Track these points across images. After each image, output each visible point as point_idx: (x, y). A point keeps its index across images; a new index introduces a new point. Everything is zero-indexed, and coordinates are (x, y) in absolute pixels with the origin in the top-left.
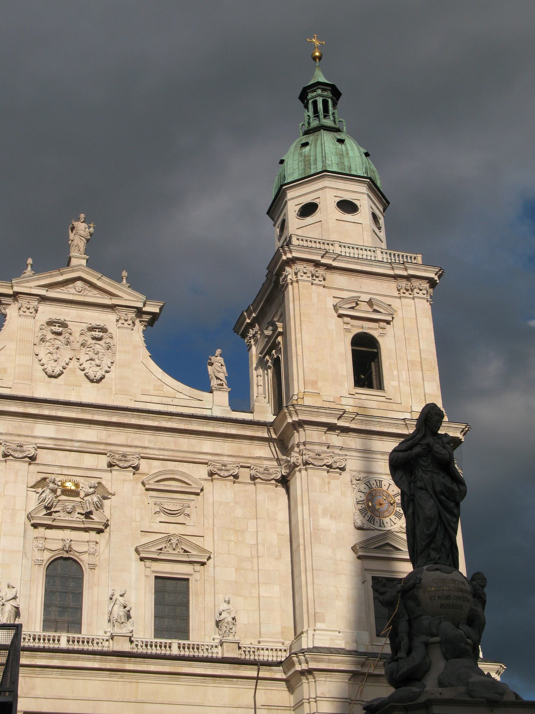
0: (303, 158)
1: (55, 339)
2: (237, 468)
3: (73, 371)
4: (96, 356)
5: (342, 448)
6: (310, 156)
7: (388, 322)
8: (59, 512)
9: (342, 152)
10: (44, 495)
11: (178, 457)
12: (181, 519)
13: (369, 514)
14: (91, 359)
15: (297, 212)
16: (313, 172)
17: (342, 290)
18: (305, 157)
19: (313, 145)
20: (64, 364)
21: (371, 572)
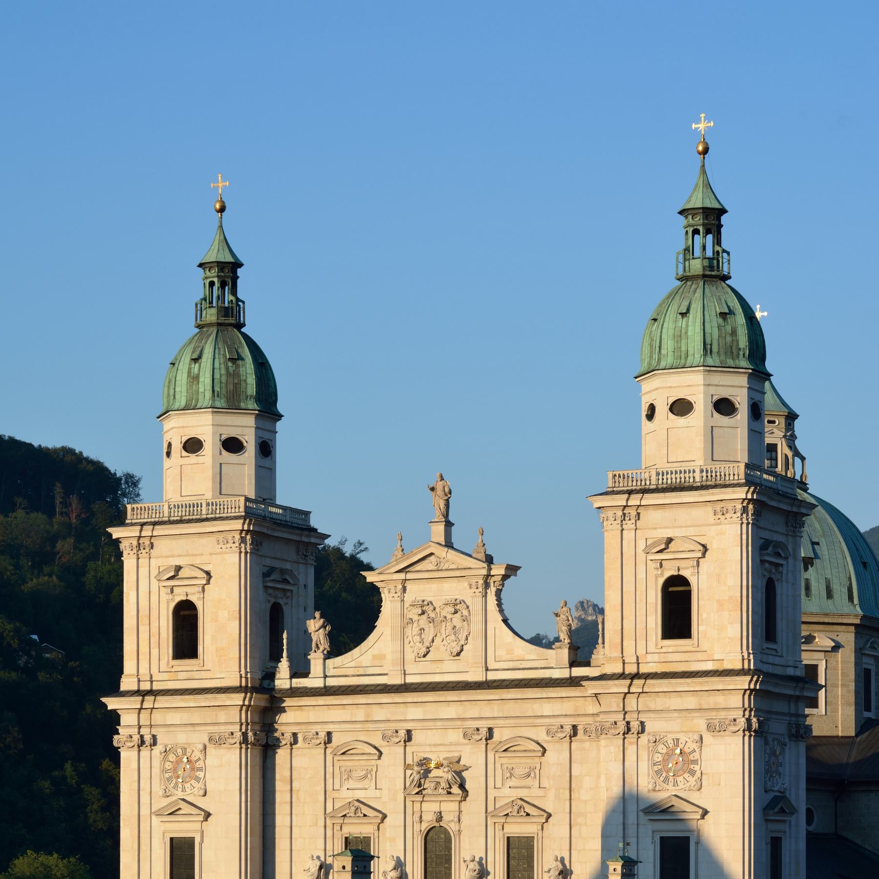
3: (438, 649)
12: (528, 782)
13: (664, 775)
20: (428, 644)
21: (659, 833)
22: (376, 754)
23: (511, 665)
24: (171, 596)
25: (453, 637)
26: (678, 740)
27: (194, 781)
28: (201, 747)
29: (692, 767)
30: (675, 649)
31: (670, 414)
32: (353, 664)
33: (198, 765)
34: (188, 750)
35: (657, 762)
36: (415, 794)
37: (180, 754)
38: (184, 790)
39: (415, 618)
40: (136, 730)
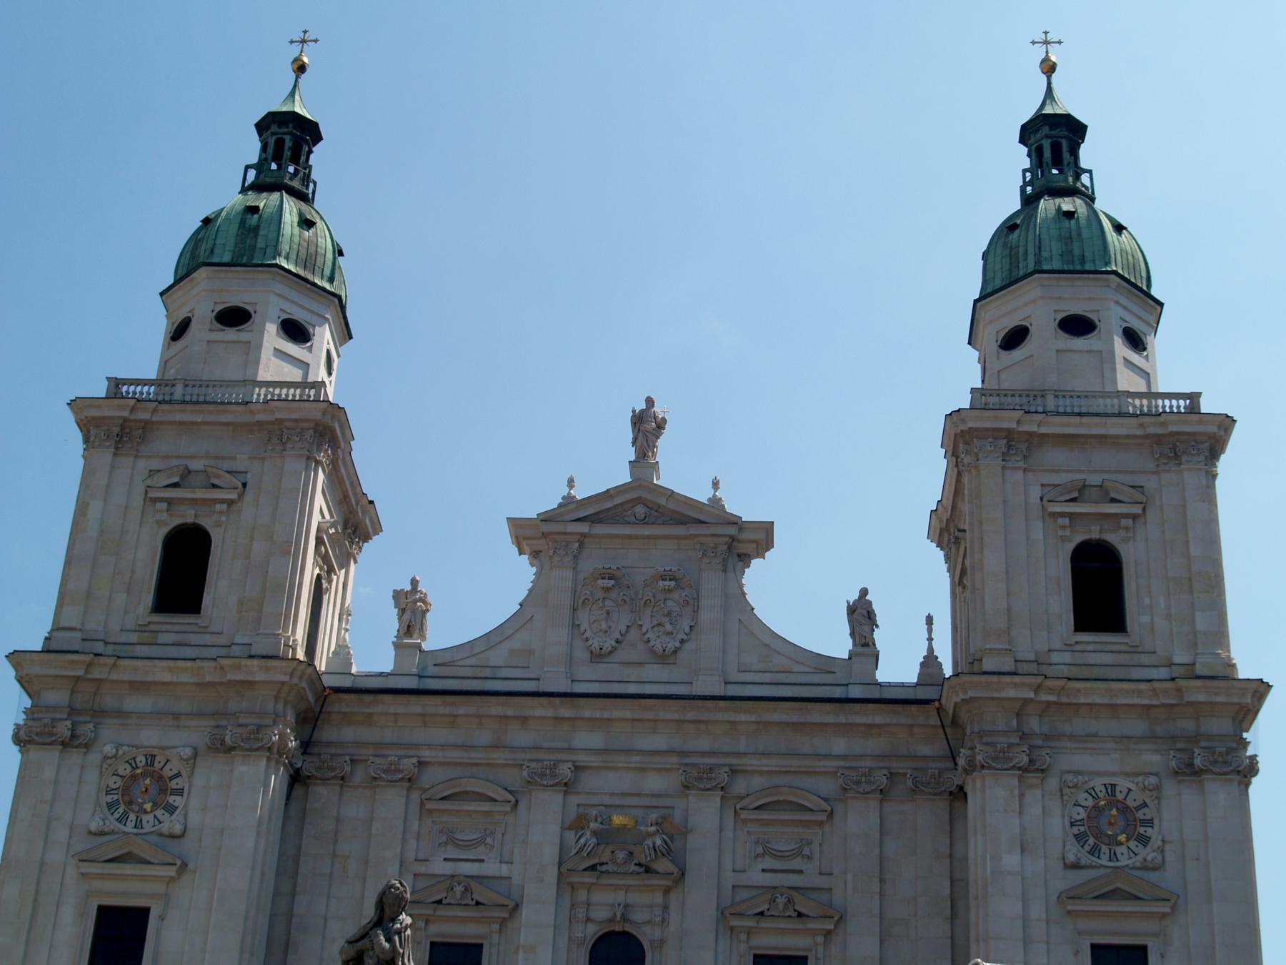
0: (1008, 251)
1: (604, 598)
2: (885, 777)
4: (666, 620)
5: (1046, 737)
6: (1018, 247)
7: (1134, 517)
8: (607, 863)
9: (1070, 232)
10: (582, 841)
11: (791, 766)
12: (796, 864)
13: (1091, 841)
14: (660, 625)
15: (999, 343)
16: (1021, 273)
17: (1057, 471)
18: (1011, 246)
19: (1023, 228)
20: (617, 635)
22: (510, 802)
23: (768, 677)
24: (165, 516)
25: (669, 627)
26: (1113, 786)
27: (163, 811)
28: (188, 752)
29: (1142, 830)
30: (1099, 647)
31: (1061, 333)
32: (468, 662)
33: (173, 784)
34: (157, 759)
35: (1077, 821)
36: (586, 870)
37: (139, 765)
38: (138, 824)
39: (600, 594)
40: (65, 716)
